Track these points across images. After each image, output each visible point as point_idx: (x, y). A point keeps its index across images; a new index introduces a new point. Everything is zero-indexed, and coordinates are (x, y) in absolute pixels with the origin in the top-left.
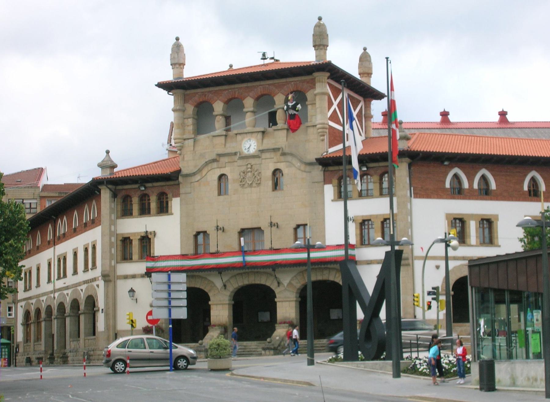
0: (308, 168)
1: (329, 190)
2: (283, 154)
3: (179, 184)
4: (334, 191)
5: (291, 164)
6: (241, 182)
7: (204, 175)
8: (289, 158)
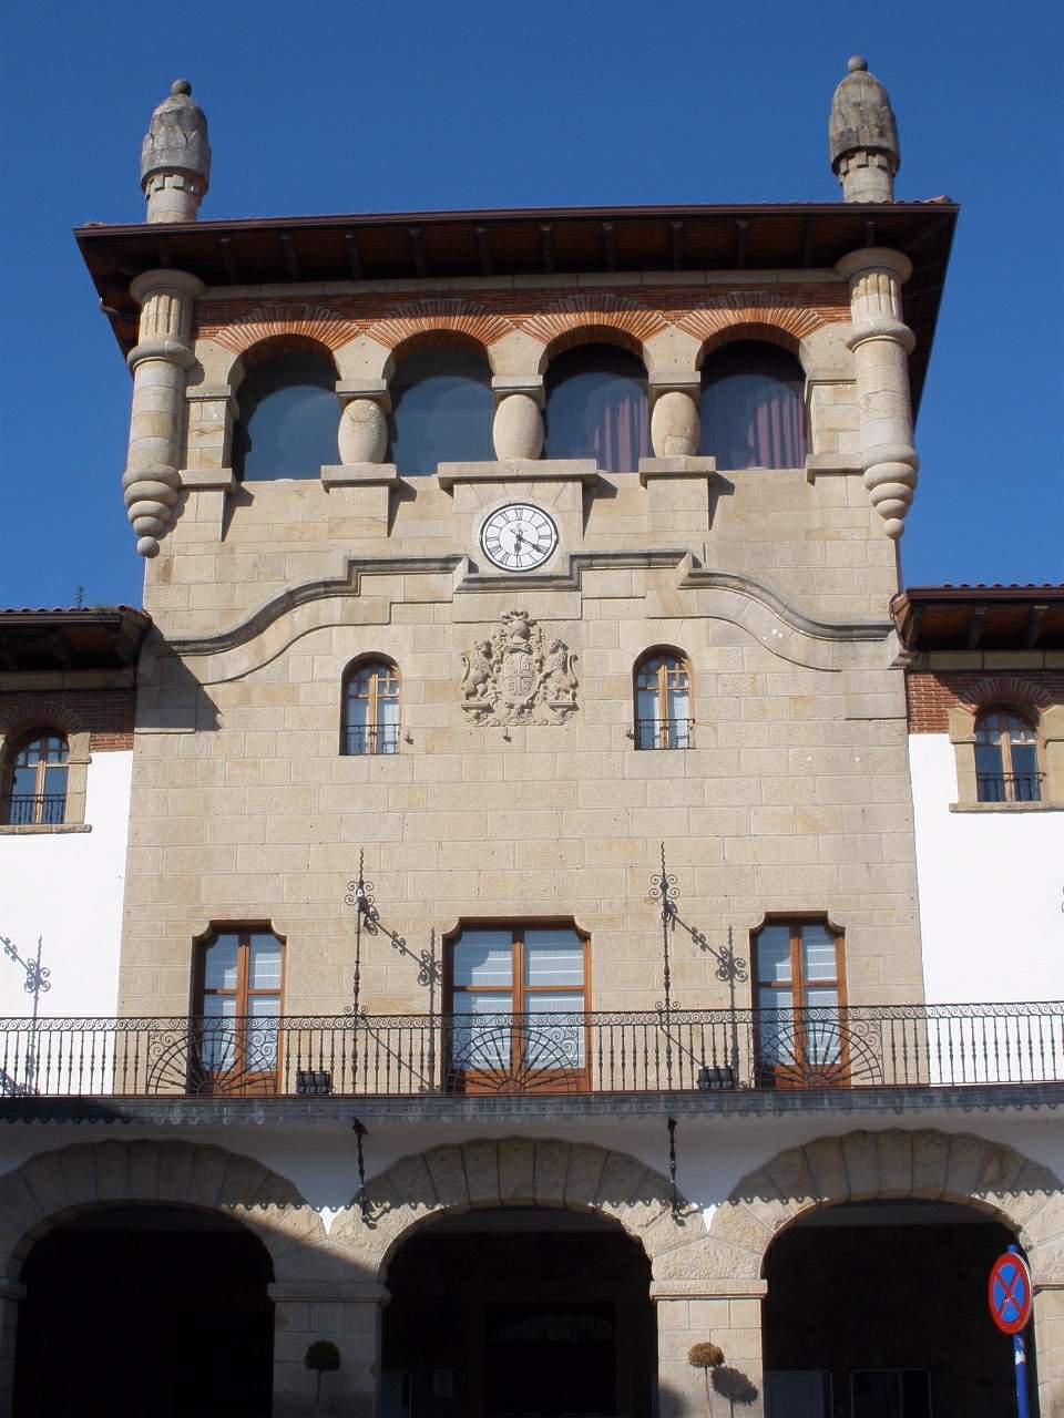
0: (826, 650)
1: (938, 761)
2: (700, 579)
3: (135, 687)
4: (960, 763)
5: (733, 630)
6: (468, 695)
7: (271, 651)
8: (726, 600)
